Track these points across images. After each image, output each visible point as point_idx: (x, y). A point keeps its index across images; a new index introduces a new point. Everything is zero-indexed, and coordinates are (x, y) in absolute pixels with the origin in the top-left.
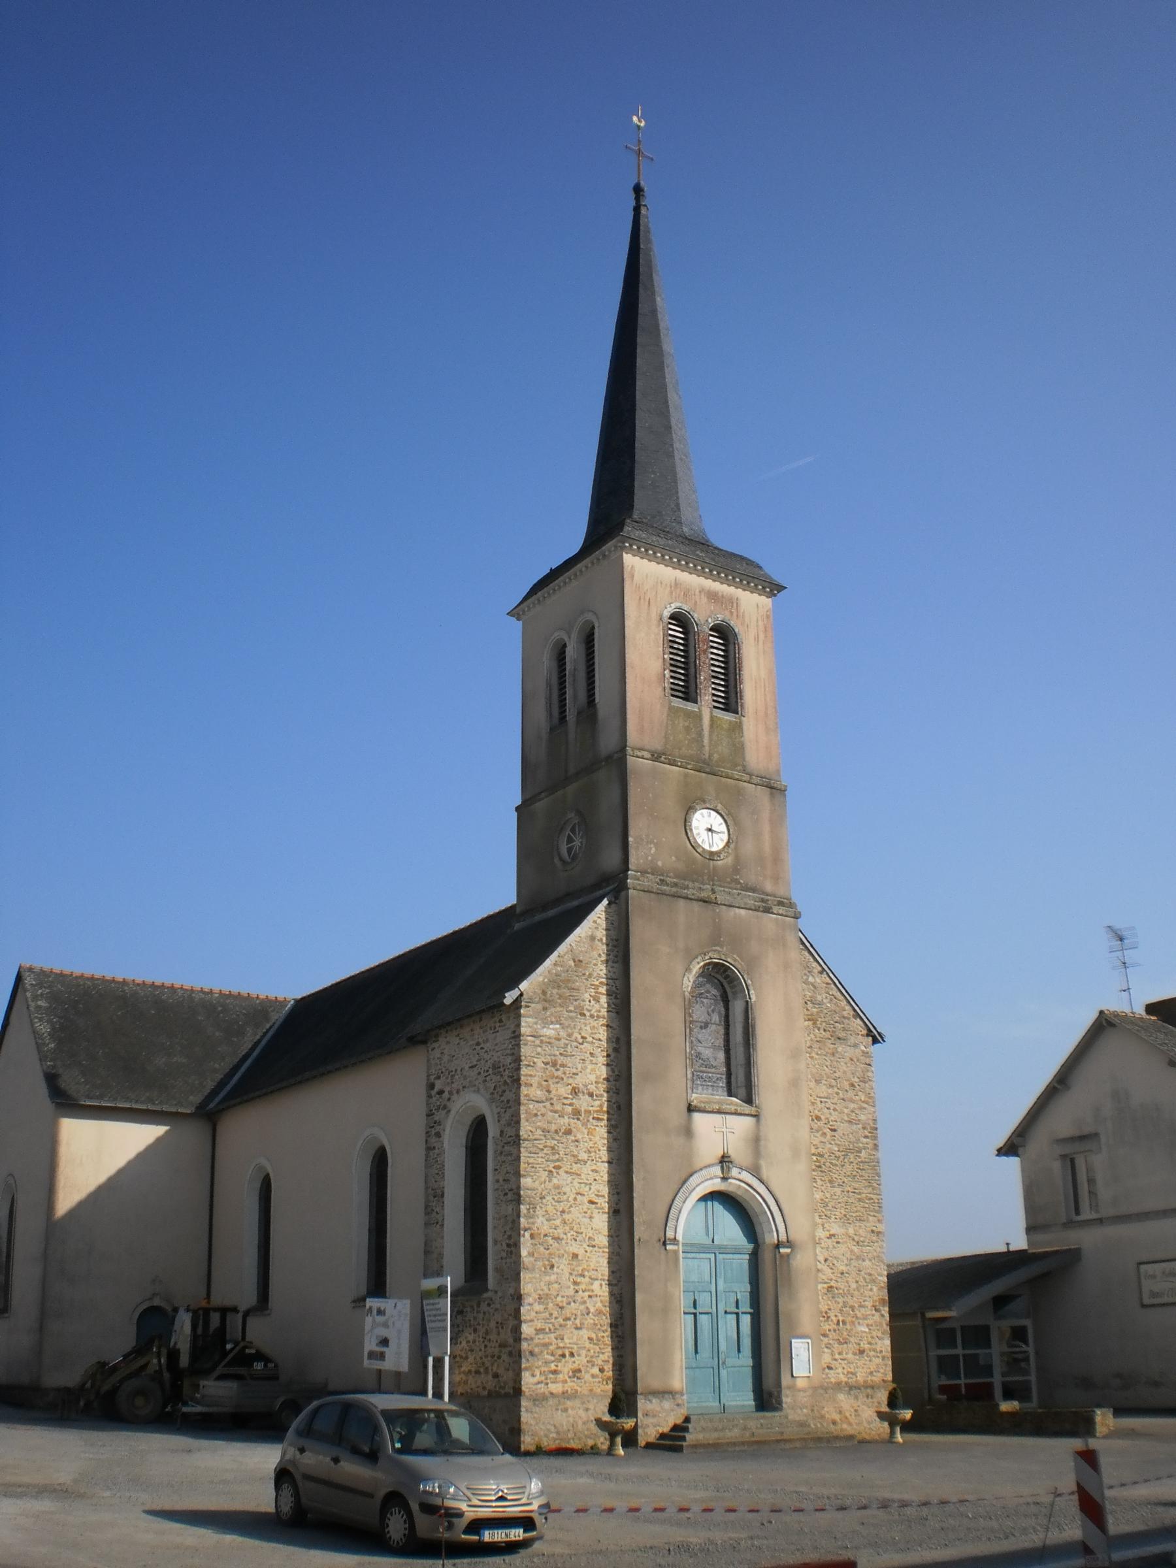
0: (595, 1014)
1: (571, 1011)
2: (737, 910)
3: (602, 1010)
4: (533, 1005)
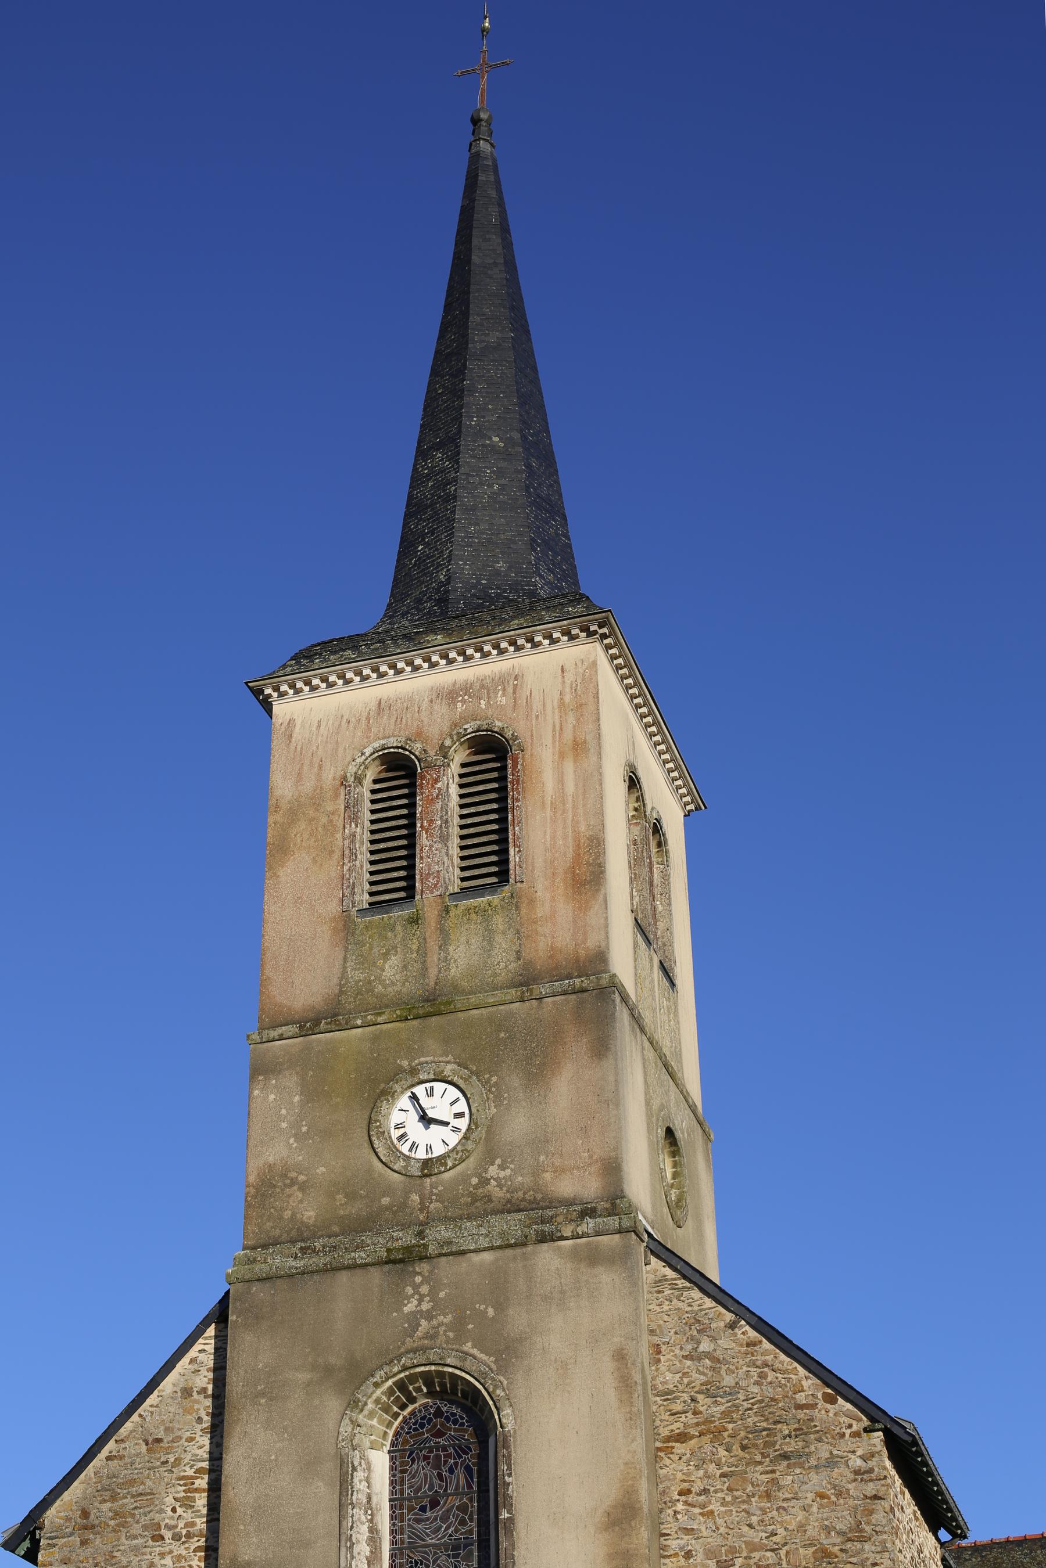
0: (184, 1532)
1: (135, 1537)
2: (476, 1258)
3: (198, 1521)
4: (60, 1542)
